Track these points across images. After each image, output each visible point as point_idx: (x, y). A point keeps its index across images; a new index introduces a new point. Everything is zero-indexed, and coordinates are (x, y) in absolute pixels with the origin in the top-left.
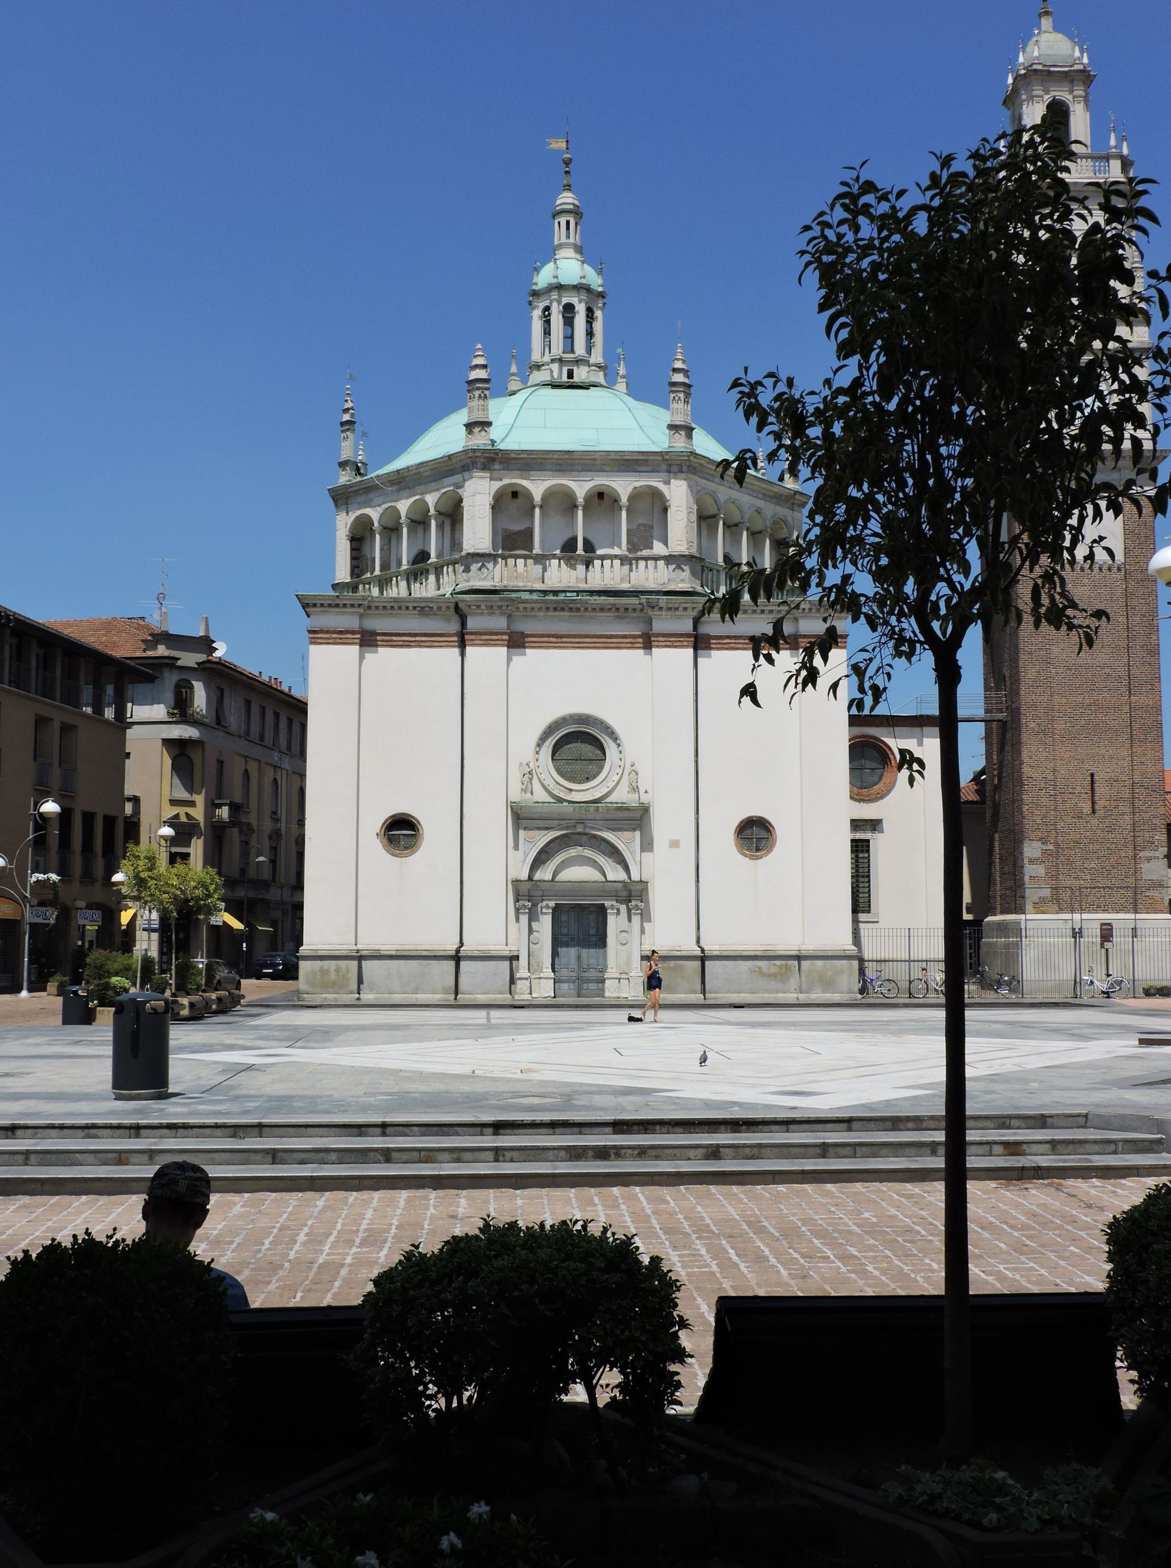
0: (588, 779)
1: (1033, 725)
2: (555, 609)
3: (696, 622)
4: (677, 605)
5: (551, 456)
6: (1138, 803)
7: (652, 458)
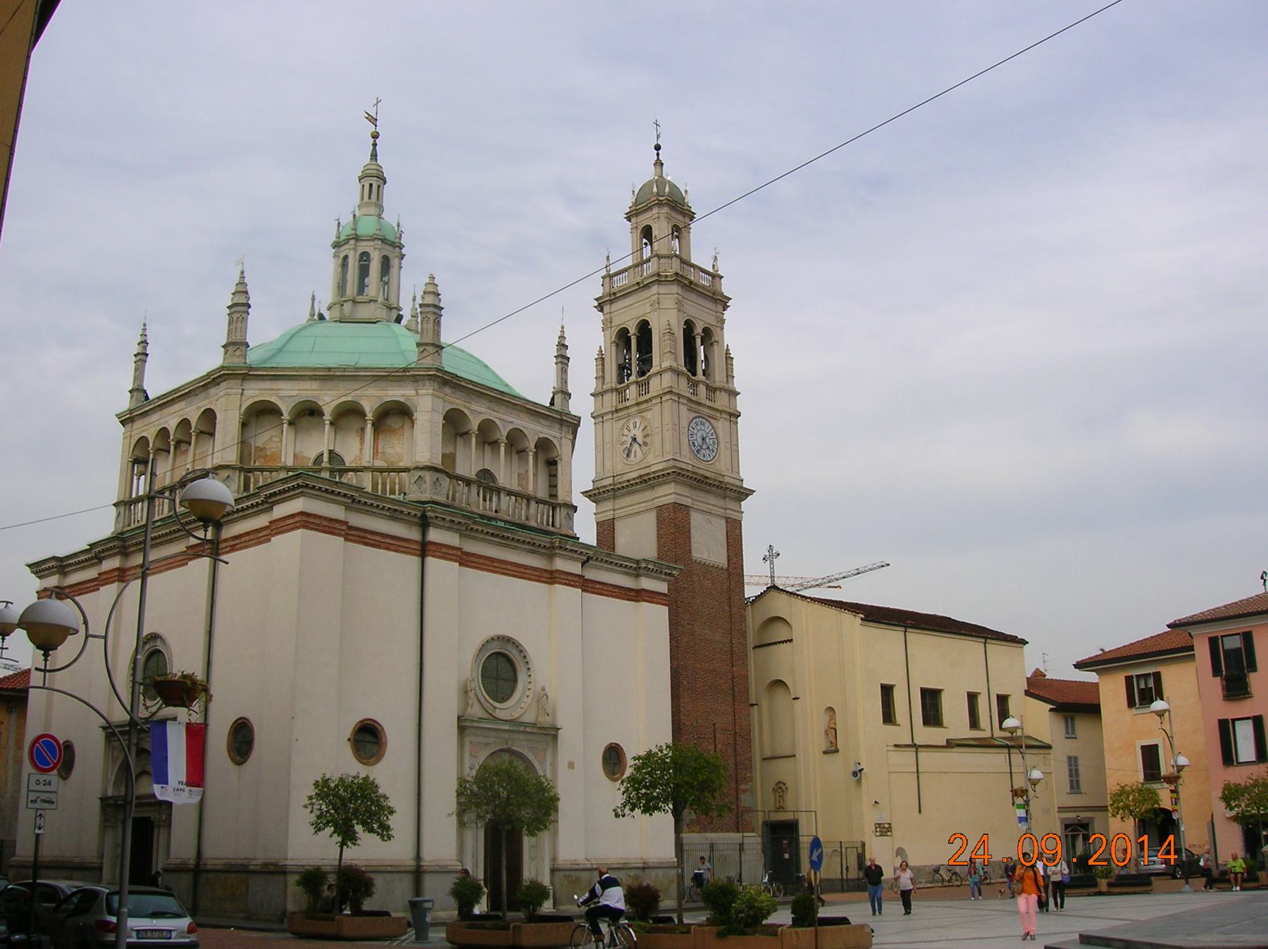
0: (503, 700)
1: (685, 683)
2: (492, 534)
3: (583, 564)
4: (577, 549)
5: (489, 393)
6: (738, 748)
7: (554, 416)
